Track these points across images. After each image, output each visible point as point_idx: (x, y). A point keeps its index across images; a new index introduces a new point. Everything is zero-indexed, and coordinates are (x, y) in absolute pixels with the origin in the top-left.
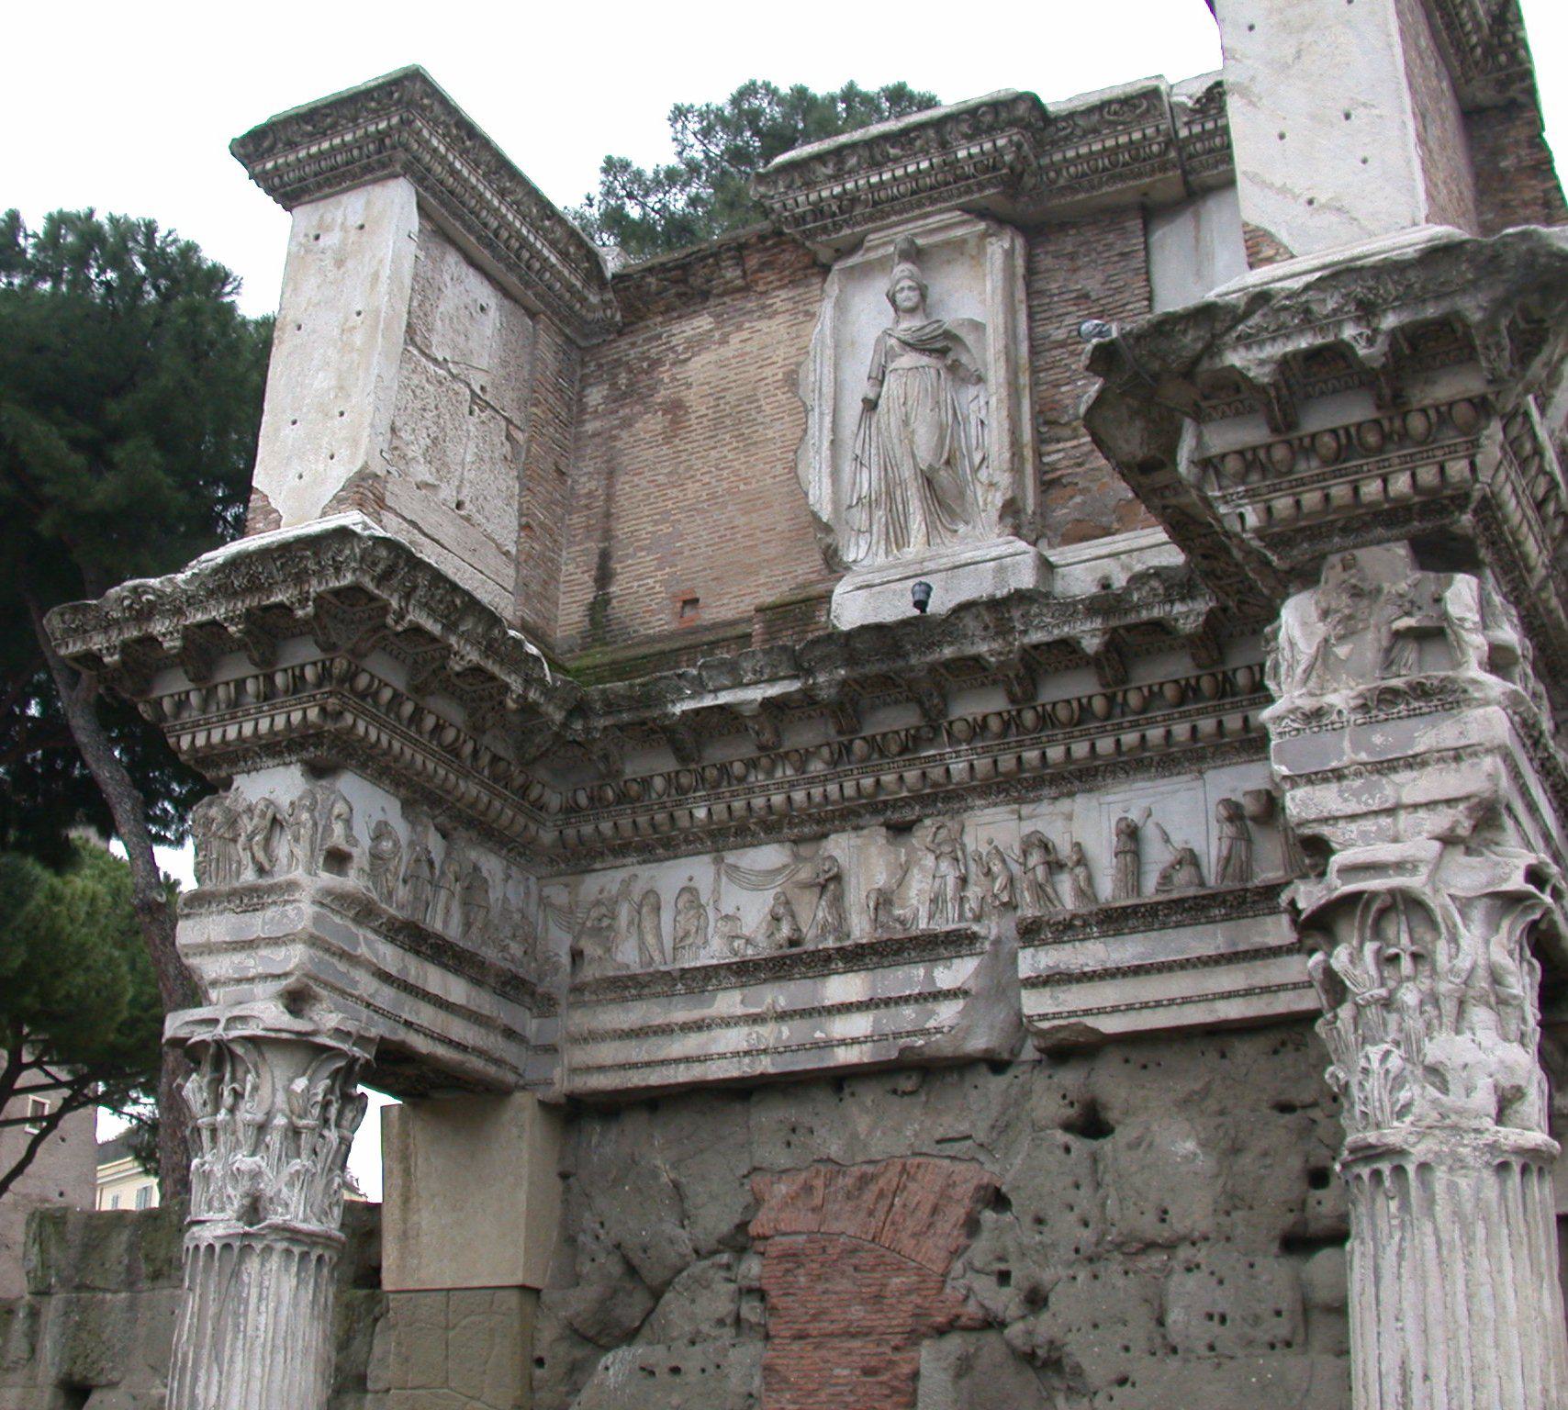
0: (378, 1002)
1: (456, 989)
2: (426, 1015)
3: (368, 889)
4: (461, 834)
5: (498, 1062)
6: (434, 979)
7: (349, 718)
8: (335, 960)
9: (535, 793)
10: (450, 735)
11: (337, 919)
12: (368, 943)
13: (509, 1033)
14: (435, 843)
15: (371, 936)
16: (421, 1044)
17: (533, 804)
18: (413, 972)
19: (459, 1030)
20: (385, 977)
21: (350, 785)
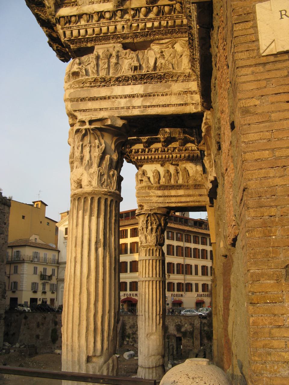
0: (159, 201)
1: (181, 192)
2: (173, 199)
3: (147, 184)
4: (180, 163)
5: (199, 202)
6: (173, 192)
7: (136, 158)
8: (146, 198)
9: (190, 148)
10: (160, 149)
11: (144, 191)
12: (152, 192)
13: (201, 195)
14: (172, 169)
15: (153, 191)
16: (173, 205)
17: (191, 151)
18: (166, 193)
19: (183, 199)
20: (160, 197)
21: (146, 167)
